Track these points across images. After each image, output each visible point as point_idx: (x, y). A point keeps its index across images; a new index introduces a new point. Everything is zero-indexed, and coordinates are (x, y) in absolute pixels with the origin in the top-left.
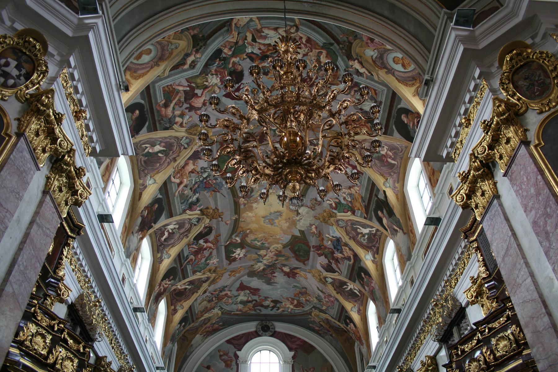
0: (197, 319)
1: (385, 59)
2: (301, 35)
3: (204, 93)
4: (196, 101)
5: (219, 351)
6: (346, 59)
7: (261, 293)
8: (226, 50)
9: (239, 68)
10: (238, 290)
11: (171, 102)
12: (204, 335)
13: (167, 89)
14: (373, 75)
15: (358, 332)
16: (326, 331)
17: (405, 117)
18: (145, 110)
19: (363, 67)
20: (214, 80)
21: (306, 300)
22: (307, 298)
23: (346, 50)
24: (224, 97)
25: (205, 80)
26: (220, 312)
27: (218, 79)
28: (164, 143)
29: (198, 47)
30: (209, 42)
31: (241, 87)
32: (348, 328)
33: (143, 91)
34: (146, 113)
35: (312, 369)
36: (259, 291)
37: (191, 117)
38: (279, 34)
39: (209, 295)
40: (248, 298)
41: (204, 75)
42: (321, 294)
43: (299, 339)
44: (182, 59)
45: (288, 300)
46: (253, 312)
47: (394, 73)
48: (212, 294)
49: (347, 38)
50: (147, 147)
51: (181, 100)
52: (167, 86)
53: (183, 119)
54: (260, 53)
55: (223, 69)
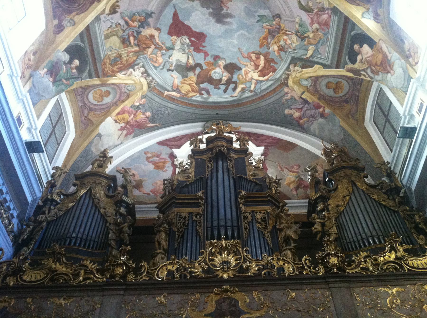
0: (106, 75)
5: (145, 153)
7: (208, 45)
10: (170, 33)
12: (122, 129)
15: (380, 51)
16: (312, 112)
21: (281, 49)
22: (282, 43)
26: (144, 82)
32: (357, 66)
35: (295, 167)
36: (204, 41)
39: (122, 22)
40: (188, 58)
42: (305, 17)
43: (269, 137)
45: (250, 58)
46: (197, 98)
48: (127, 23)
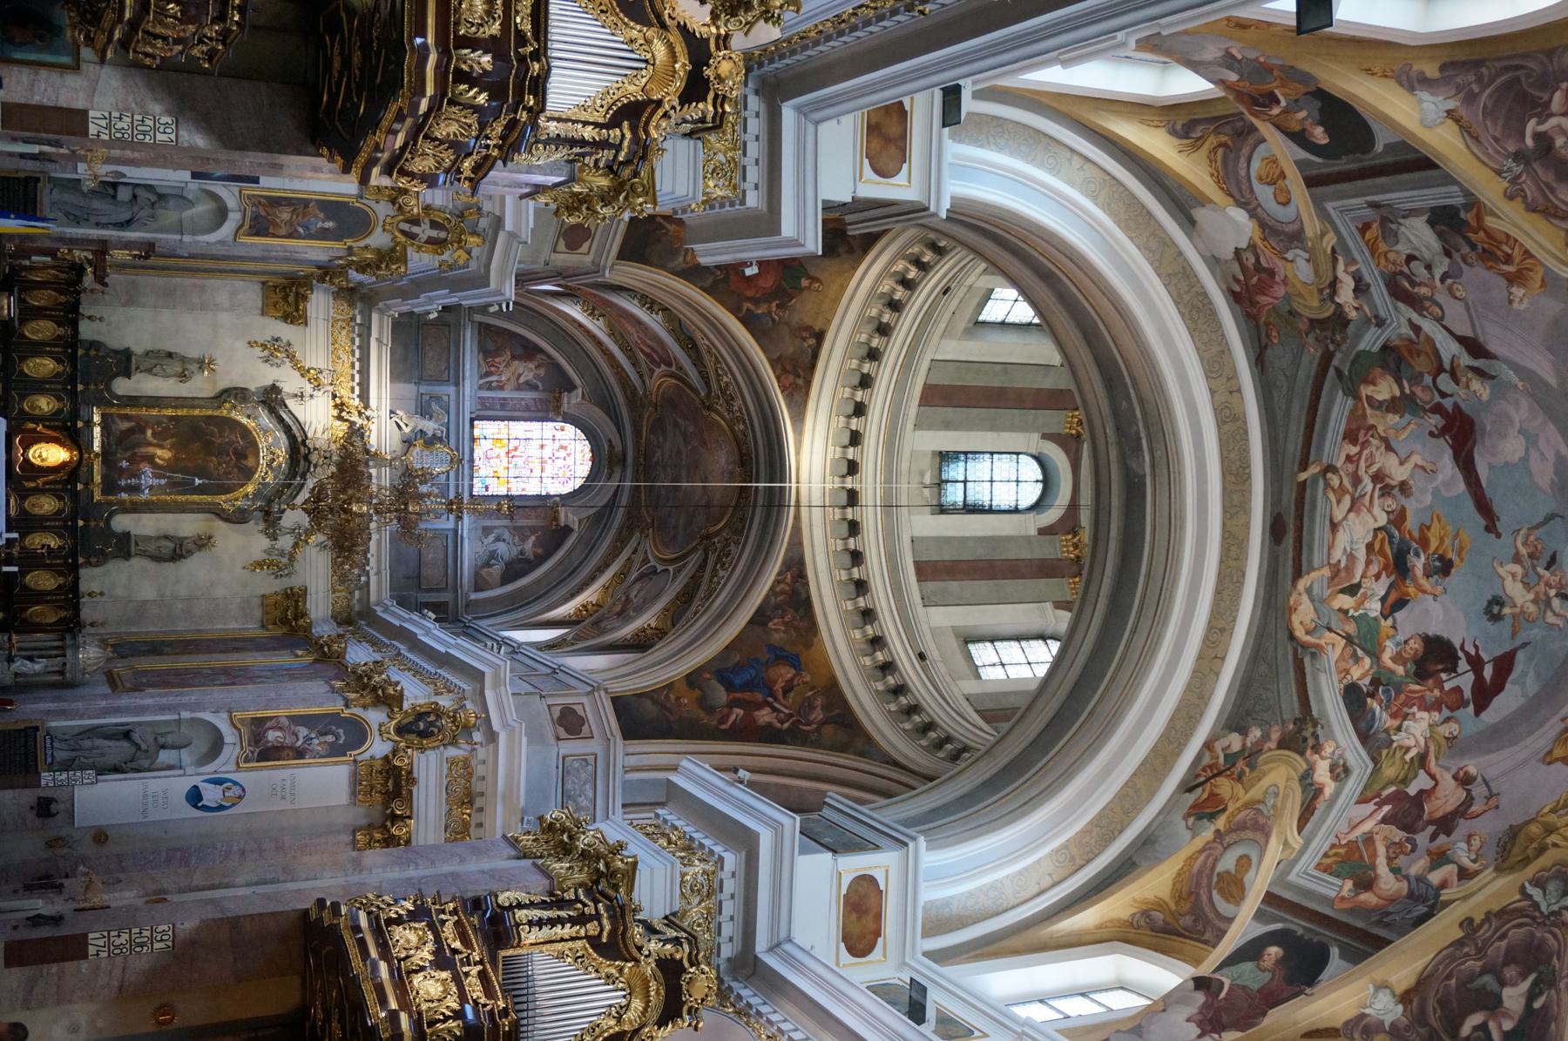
2: (1343, 458)
6: (1351, 329)
8: (1356, 673)
9: (1416, 645)
11: (1373, 867)
13: (1328, 861)
14: (1333, 248)
18: (1300, 932)
19: (1336, 278)
20: (1417, 729)
23: (1334, 334)
24: (1483, 715)
25: (1398, 754)
27: (1420, 715)
28: (1506, 964)
29: (1311, 742)
30: (1315, 713)
31: (1473, 652)
37: (1470, 836)
38: (1345, 518)
41: (1384, 752)
44: (1303, 792)
50: (1483, 1027)
51: (1397, 840)
52: (1326, 855)
53: (1449, 862)
54: (1388, 577)
55: (1398, 693)
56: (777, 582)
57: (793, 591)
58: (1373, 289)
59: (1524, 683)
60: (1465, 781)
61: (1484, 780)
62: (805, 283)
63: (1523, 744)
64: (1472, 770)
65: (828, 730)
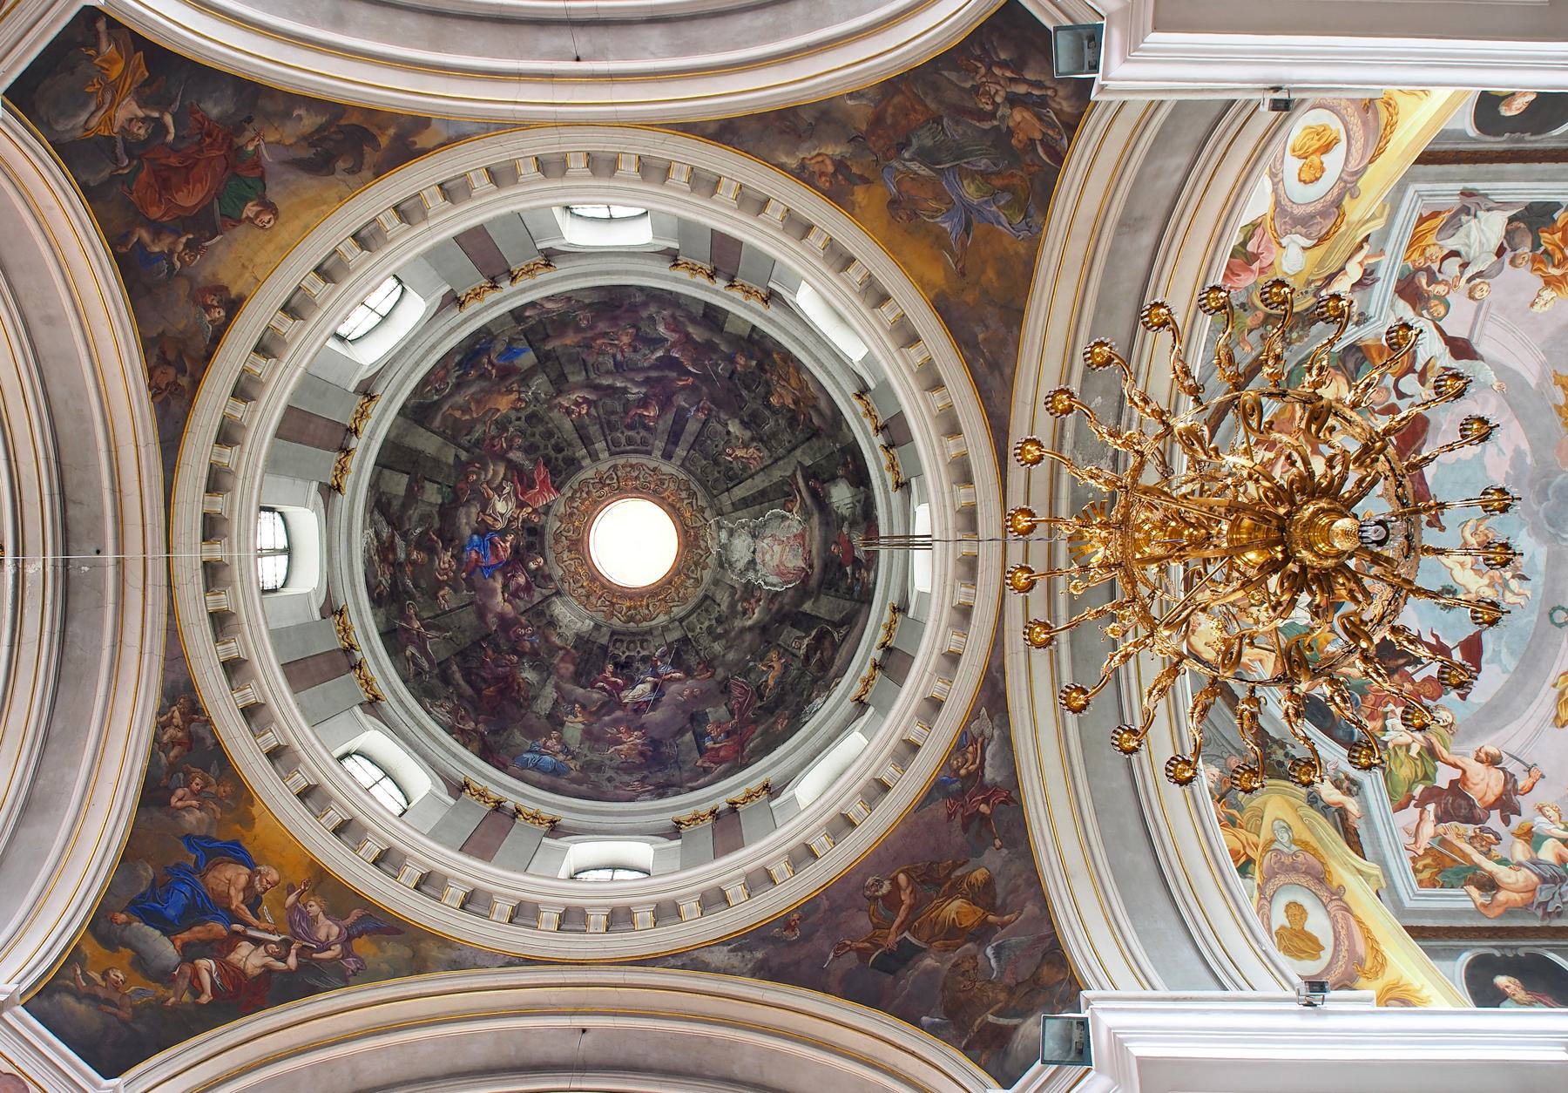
1: (1310, 209)
3: (1451, 759)
4: (1482, 786)
13: (1426, 875)
14: (1366, 239)
17: (1509, 105)
25: (1402, 753)
33: (1425, 949)
34: (1510, 955)
37: (1540, 809)
44: (1326, 817)
47: (1355, 173)
49: (1250, 331)
51: (1471, 833)
52: (1415, 871)
56: (162, 726)
57: (190, 735)
58: (1378, 285)
59: (1500, 661)
60: (1493, 761)
61: (1511, 756)
62: (250, 210)
63: (1526, 715)
64: (1493, 750)
65: (363, 946)
